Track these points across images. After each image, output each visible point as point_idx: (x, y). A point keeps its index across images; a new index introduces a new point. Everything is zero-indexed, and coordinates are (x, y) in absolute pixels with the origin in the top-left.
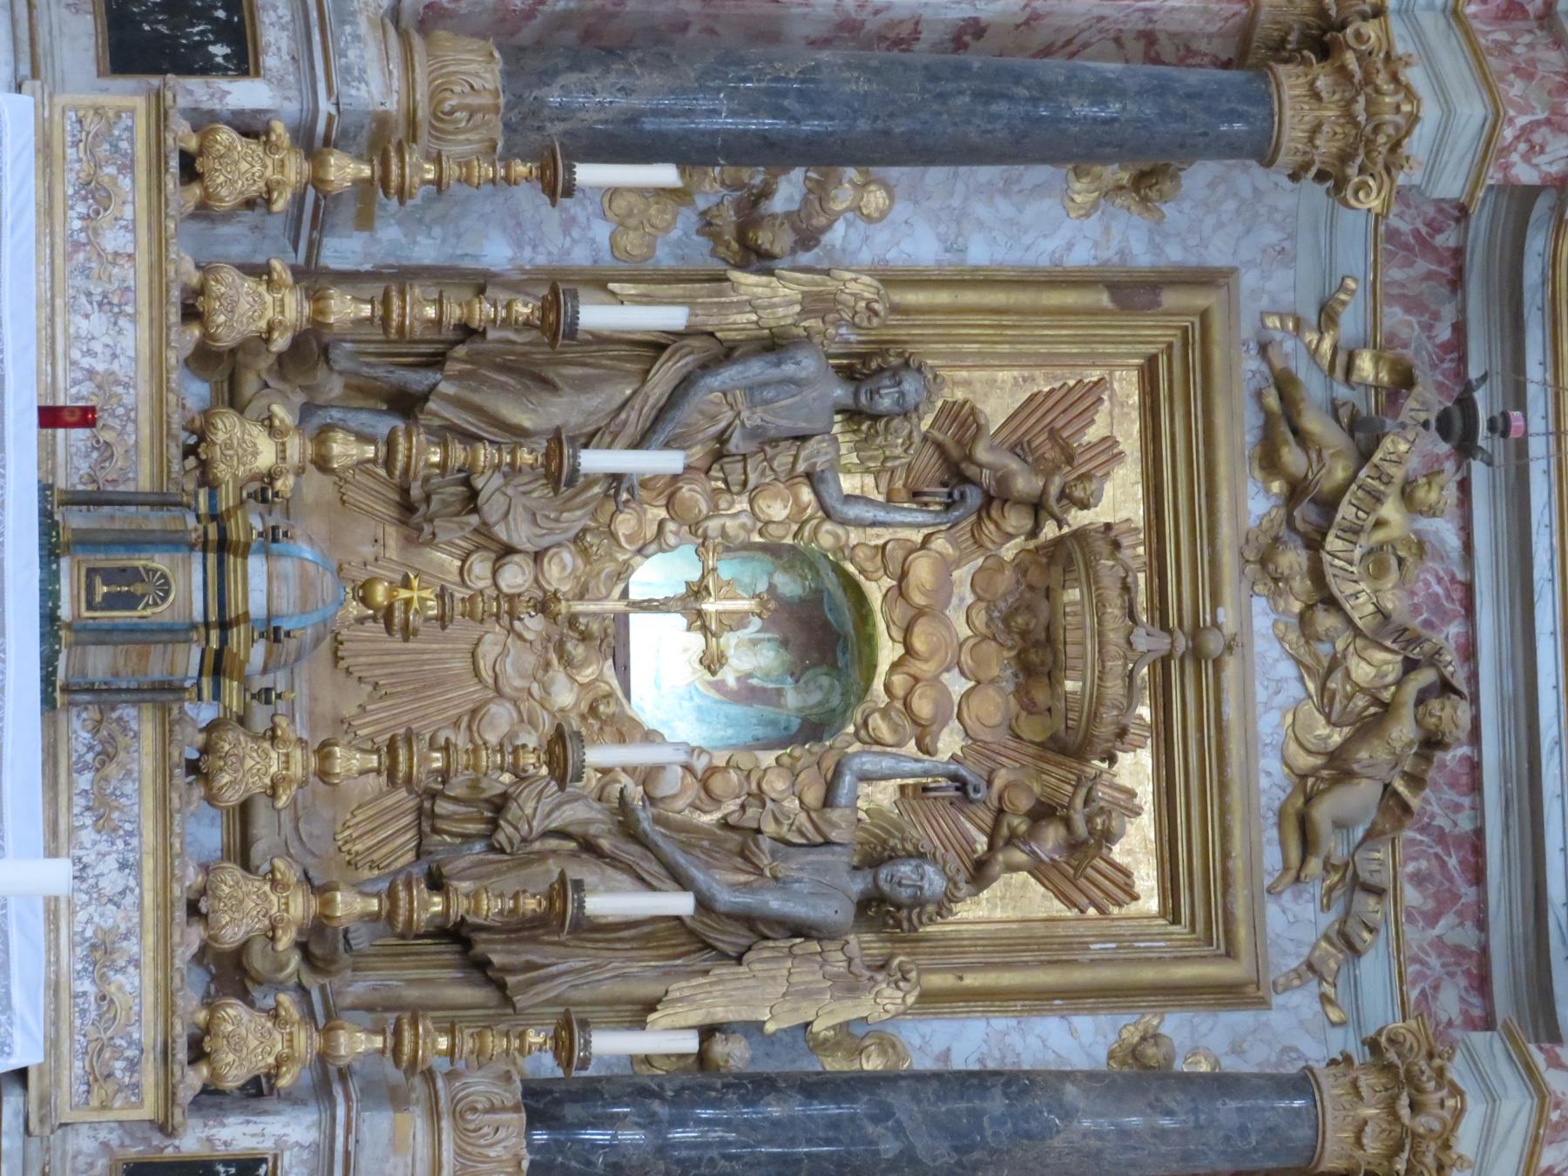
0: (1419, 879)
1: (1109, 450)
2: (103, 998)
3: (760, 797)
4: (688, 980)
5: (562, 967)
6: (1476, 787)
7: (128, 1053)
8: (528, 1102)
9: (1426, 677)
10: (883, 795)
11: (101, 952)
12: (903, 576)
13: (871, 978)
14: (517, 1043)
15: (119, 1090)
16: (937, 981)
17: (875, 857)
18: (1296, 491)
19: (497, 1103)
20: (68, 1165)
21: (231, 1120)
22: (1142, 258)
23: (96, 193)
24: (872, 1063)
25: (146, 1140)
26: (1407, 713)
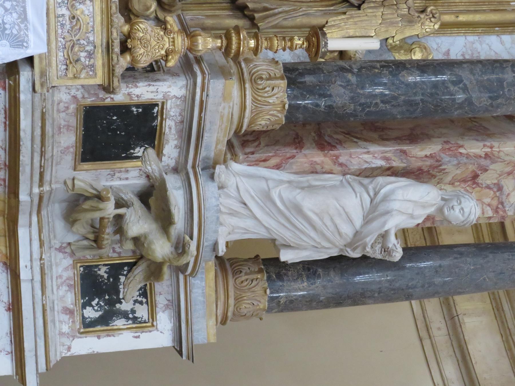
2: (74, 17)
4: (336, 16)
5: (280, 10)
7: (88, 48)
8: (287, 74)
13: (419, 17)
14: (289, 44)
15: (84, 68)
16: (448, 18)
19: (272, 75)
20: (55, 108)
21: (140, 84)
24: (417, 56)
25: (96, 95)
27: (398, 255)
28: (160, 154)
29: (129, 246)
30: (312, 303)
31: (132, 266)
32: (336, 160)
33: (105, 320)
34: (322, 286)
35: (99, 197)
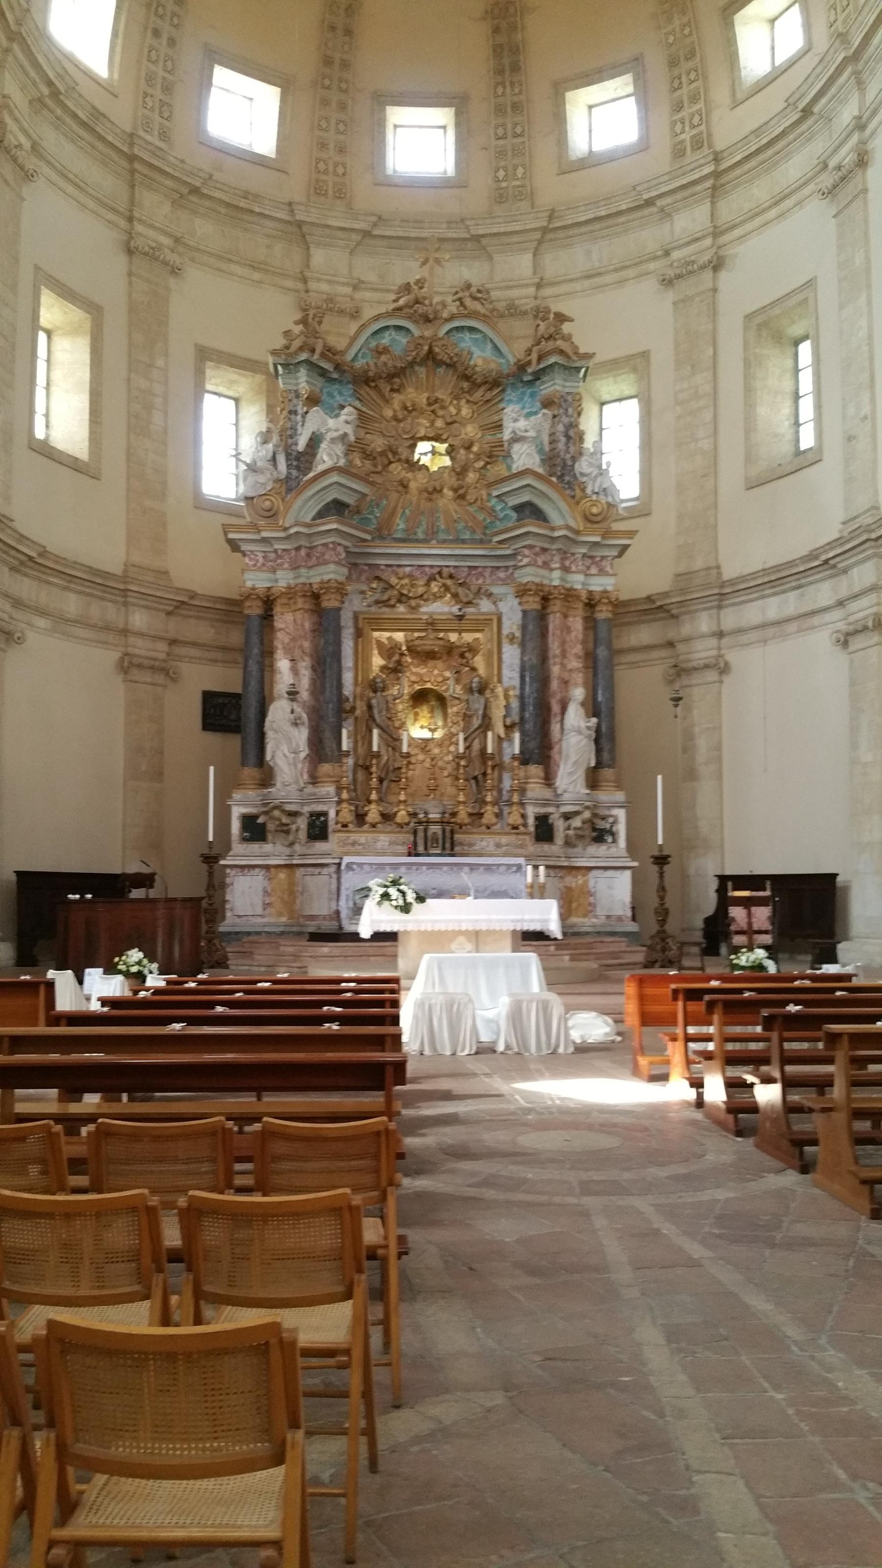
0: (477, 579)
11: (498, 845)
12: (414, 682)
16: (495, 679)
17: (471, 691)
18: (399, 601)
23: (353, 844)
27: (594, 720)
29: (586, 826)
30: (612, 751)
32: (556, 743)
33: (613, 834)
34: (606, 746)
35: (567, 836)
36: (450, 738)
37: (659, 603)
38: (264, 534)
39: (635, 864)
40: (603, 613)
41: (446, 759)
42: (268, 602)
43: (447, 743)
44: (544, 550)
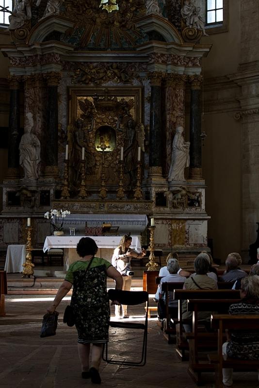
0: (131, 69)
1: (86, 100)
3: (121, 138)
6: (122, 62)
9: (110, 68)
10: (122, 126)
11: (135, 208)
16: (140, 122)
18: (90, 80)
22: (66, 96)
26: (115, 70)
28: (166, 191)
31: (188, 196)
36: (116, 151)
37: (231, 79)
38: (19, 49)
39: (210, 217)
40: (196, 87)
41: (115, 162)
42: (22, 82)
43: (115, 154)
44: (163, 55)
